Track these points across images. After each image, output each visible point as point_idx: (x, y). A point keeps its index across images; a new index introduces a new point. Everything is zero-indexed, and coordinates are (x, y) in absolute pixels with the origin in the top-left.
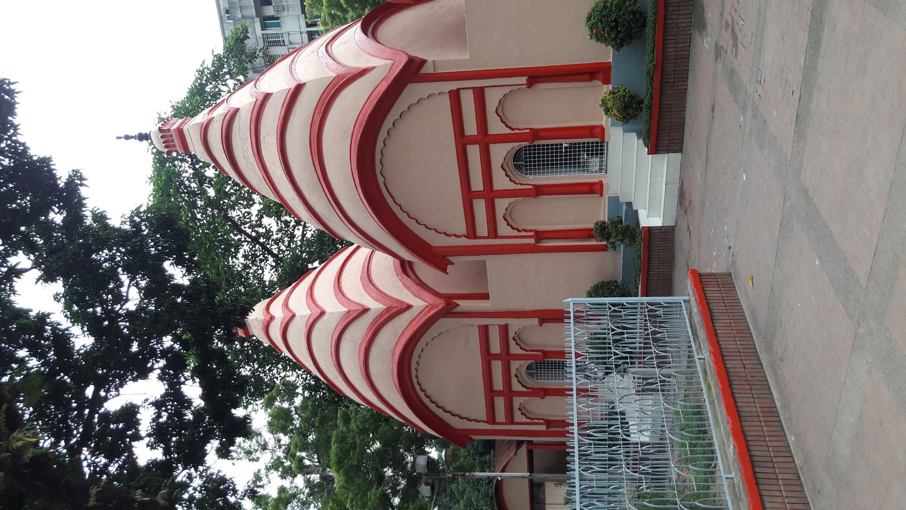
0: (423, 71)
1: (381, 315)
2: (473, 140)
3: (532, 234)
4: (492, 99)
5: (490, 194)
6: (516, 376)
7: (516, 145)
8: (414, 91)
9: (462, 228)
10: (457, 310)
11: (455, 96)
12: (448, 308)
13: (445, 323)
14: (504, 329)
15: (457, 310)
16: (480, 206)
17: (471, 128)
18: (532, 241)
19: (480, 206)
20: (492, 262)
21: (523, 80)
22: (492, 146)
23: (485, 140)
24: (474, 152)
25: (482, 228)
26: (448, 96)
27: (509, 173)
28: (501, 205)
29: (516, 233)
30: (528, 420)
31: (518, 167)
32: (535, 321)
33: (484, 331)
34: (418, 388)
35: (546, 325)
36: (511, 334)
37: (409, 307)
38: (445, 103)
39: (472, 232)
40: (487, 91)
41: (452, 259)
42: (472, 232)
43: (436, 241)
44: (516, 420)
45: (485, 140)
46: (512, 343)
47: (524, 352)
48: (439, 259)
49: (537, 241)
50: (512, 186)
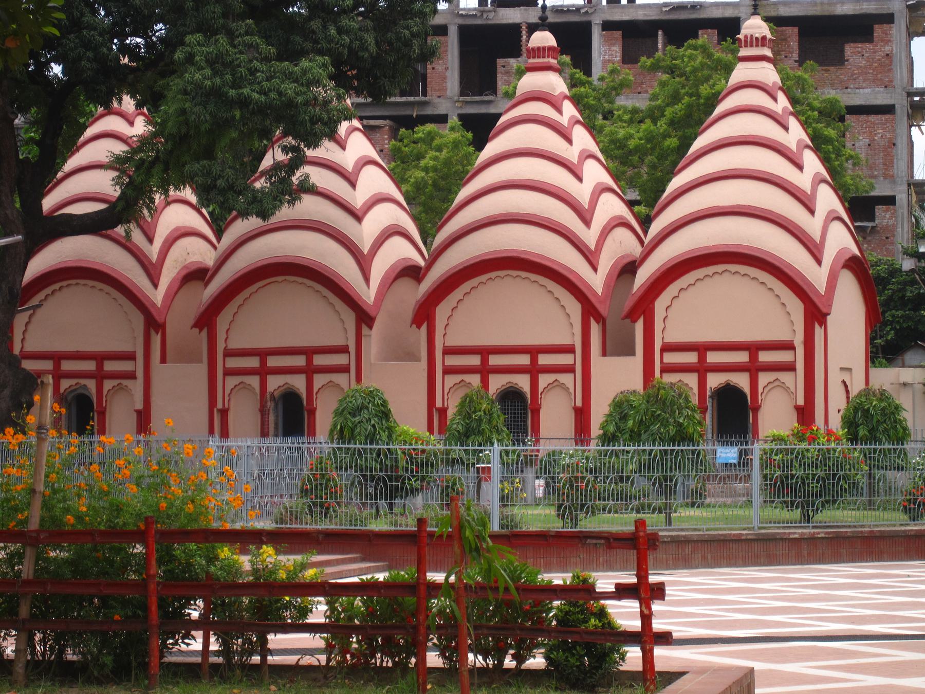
1: (146, 256)
3: (226, 406)
5: (263, 372)
7: (304, 396)
8: (350, 318)
9: (234, 344)
10: (153, 332)
11: (344, 350)
12: (153, 323)
13: (138, 320)
14: (132, 376)
15: (153, 332)
16: (254, 362)
17: (319, 360)
18: (220, 405)
19: (254, 362)
20: (201, 369)
23: (310, 371)
25: (233, 363)
26: (344, 344)
28: (254, 381)
32: (139, 405)
33: (130, 356)
34: (64, 283)
35: (135, 415)
36: (125, 382)
37: (156, 286)
38: (338, 341)
39: (229, 353)
40: (346, 375)
41: (205, 333)
42: (229, 353)
43: (223, 321)
45: (310, 371)
47: (105, 393)
48: (206, 320)
49: (219, 410)
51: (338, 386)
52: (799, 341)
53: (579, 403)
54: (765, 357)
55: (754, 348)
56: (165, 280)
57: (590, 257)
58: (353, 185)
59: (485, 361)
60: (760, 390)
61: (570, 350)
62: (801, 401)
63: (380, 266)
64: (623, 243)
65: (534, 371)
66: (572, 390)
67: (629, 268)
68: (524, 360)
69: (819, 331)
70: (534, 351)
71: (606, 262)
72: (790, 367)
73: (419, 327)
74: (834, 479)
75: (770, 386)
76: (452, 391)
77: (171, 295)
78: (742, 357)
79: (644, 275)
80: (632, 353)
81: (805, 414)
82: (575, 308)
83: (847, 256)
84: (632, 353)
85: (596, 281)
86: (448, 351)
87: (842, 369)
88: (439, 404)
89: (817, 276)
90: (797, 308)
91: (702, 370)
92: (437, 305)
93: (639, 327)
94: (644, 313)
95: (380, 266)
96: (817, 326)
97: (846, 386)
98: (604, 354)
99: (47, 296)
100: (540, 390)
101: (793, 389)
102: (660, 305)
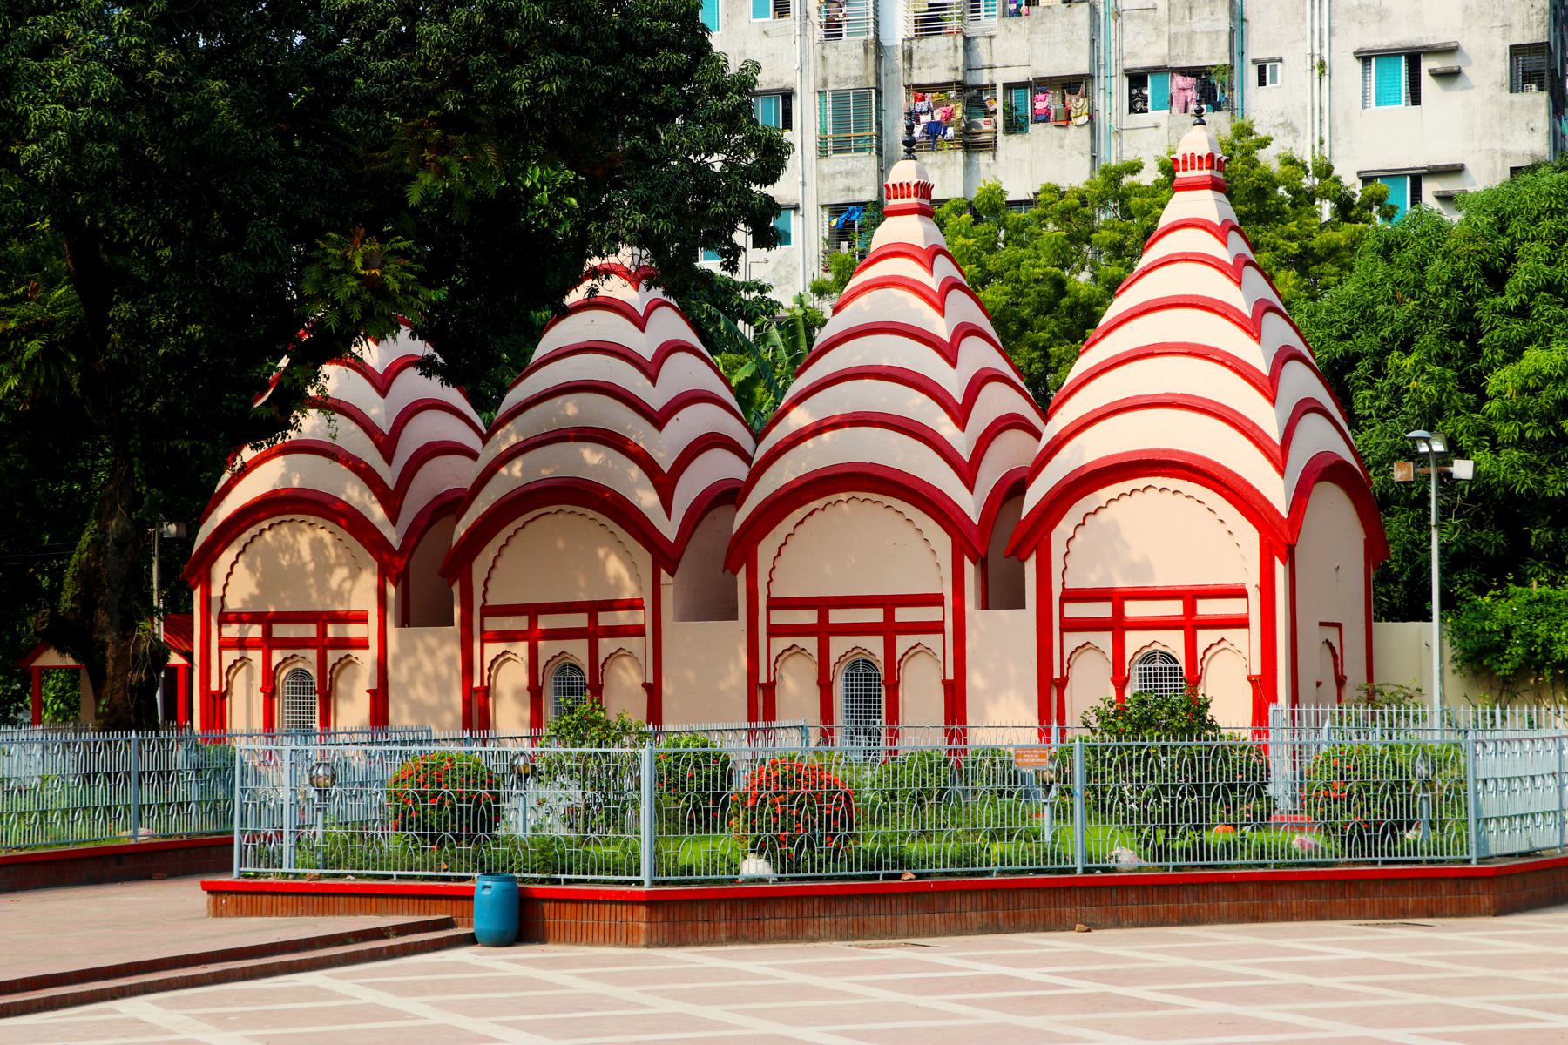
0: (663, 572)
2: (593, 619)
4: (633, 644)
6: (293, 656)
8: (645, 558)
9: (492, 601)
14: (363, 644)
21: (650, 680)
22: (585, 642)
23: (593, 634)
24: (580, 620)
29: (487, 664)
30: (225, 670)
36: (355, 653)
39: (488, 611)
42: (488, 611)
44: (225, 652)
46: (342, 653)
51: (630, 654)
52: (1252, 581)
53: (950, 676)
54: (1205, 608)
55: (1190, 597)
56: (408, 514)
57: (968, 473)
58: (654, 380)
59: (823, 617)
60: (1200, 656)
61: (936, 600)
62: (1257, 670)
63: (688, 490)
64: (1011, 451)
65: (889, 630)
67: (1014, 486)
68: (876, 615)
69: (1280, 570)
70: (889, 603)
71: (990, 474)
72: (1241, 623)
73: (735, 572)
74: (716, 803)
75: (1214, 649)
77: (415, 534)
78: (1175, 608)
79: (1035, 494)
80: (1021, 604)
81: (1263, 689)
82: (942, 542)
83: (1332, 461)
84: (1021, 604)
85: (971, 504)
86: (776, 604)
87: (1321, 624)
88: (763, 679)
89: (1276, 491)
90: (1249, 536)
92: (758, 542)
93: (1030, 567)
94: (1035, 548)
95: (688, 490)
96: (1278, 562)
97: (1332, 649)
98: (985, 605)
99: (253, 538)
100: (898, 657)
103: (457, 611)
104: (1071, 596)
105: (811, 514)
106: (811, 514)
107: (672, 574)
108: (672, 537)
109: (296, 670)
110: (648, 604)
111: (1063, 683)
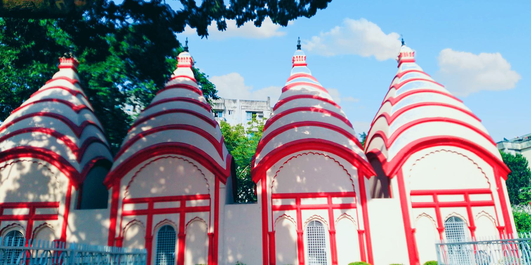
6: (13, 224)
8: (211, 177)
23: (183, 211)
24: (177, 204)
27: (161, 223)
31: (163, 228)
36: (49, 222)
40: (208, 212)
46: (41, 222)
49: (117, 239)
50: (154, 224)
52: (494, 188)
54: (473, 198)
55: (466, 193)
66: (356, 219)
76: (277, 221)
78: (460, 198)
88: (270, 230)
90: (489, 170)
91: (437, 206)
94: (397, 173)
101: (495, 218)
102: (406, 168)
103: (110, 201)
104: (413, 194)
105: (290, 159)
106: (290, 159)
107: (224, 183)
108: (225, 168)
109: (13, 232)
110: (213, 197)
111: (413, 231)
